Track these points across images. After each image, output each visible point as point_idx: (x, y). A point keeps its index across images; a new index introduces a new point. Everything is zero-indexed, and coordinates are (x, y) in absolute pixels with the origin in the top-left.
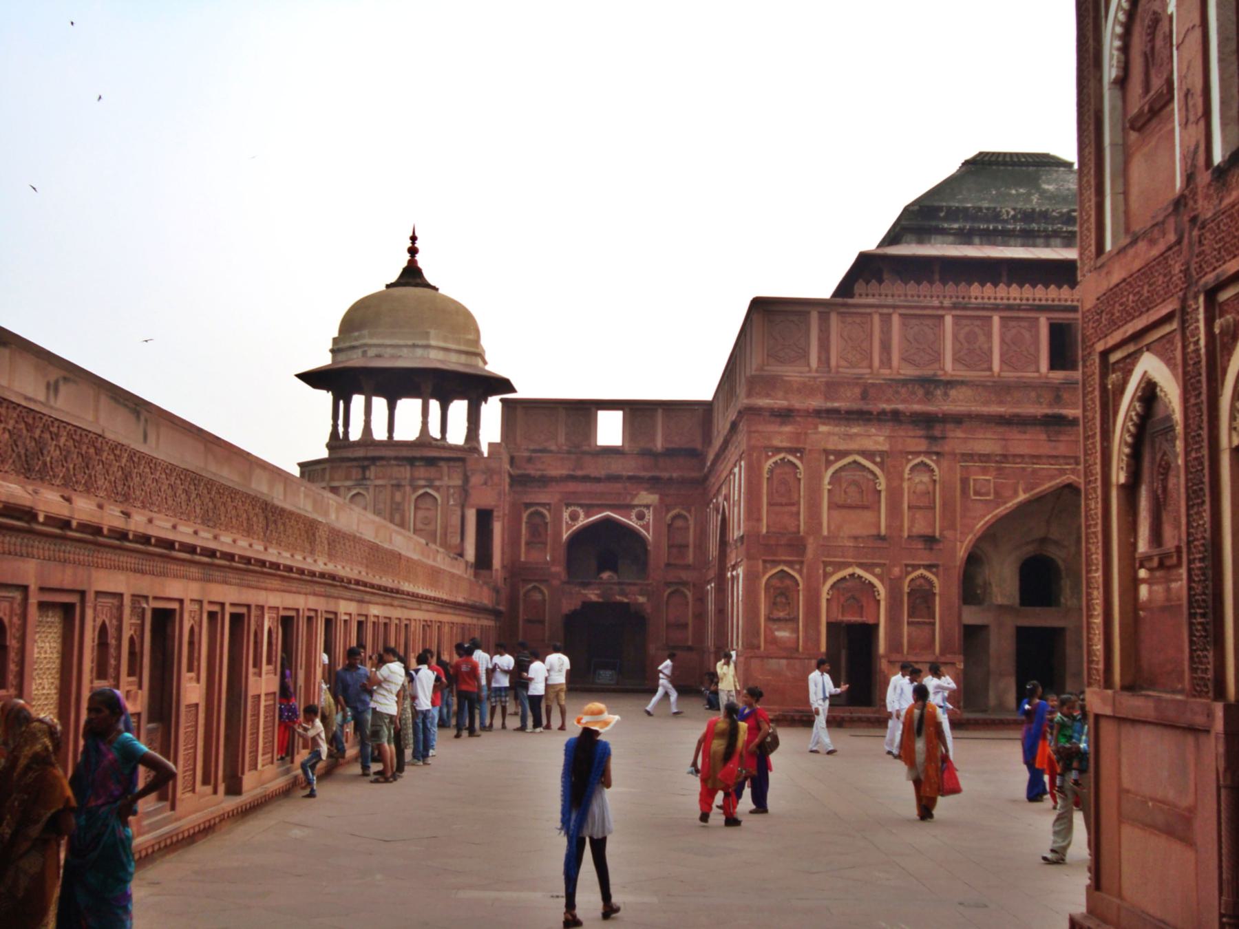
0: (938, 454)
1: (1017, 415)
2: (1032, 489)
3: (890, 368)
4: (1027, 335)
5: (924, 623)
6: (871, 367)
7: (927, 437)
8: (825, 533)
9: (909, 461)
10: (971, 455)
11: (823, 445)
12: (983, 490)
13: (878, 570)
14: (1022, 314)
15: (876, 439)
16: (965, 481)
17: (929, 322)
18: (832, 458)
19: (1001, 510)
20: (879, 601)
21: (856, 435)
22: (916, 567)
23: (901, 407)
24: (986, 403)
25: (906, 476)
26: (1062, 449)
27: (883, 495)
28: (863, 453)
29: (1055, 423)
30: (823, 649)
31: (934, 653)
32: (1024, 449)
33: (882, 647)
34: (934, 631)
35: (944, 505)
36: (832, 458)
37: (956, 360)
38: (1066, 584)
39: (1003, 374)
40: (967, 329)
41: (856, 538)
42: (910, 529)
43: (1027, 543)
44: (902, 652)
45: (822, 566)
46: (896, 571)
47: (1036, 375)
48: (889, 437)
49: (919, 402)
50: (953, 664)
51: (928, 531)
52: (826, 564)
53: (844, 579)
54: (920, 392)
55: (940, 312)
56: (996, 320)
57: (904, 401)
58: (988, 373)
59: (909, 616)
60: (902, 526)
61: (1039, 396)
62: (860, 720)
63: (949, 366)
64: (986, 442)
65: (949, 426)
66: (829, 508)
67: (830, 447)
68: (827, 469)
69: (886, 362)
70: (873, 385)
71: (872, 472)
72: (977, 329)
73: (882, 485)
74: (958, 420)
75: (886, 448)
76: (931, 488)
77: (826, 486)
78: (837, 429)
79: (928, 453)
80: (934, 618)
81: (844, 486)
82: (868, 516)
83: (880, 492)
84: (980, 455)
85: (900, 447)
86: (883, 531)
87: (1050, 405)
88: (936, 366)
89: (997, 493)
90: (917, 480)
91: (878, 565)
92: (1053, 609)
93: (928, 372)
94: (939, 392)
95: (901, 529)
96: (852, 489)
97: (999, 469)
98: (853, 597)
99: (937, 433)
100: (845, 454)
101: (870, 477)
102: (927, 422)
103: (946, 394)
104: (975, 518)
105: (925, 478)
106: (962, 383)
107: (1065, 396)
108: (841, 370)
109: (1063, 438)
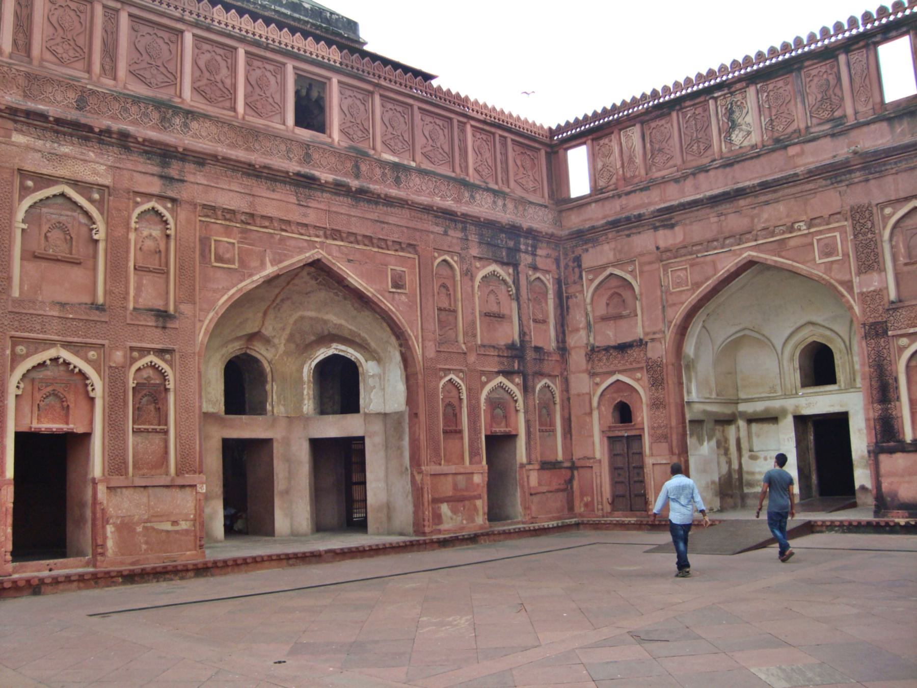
0: (173, 200)
1: (265, 167)
2: (281, 262)
3: (115, 79)
4: (272, 80)
5: (155, 431)
6: (89, 71)
7: (161, 177)
8: (16, 293)
9: (137, 204)
10: (213, 208)
11: (17, 163)
12: (228, 256)
13: (92, 354)
14: (268, 54)
15: (96, 166)
16: (204, 242)
17: (166, 35)
18: (30, 183)
19: (248, 284)
20: (92, 400)
21: (66, 156)
22: (144, 351)
23: (131, 129)
24: (233, 146)
25: (133, 225)
26: (311, 218)
27: (101, 246)
28: (75, 184)
29: (305, 183)
30: (10, 473)
31: (167, 473)
32: (271, 211)
33: (97, 466)
34: (166, 442)
35: (181, 269)
36: (30, 183)
37: (195, 89)
38: (273, 389)
39: (247, 118)
40: (208, 56)
41: (63, 305)
42: (136, 301)
43: (238, 338)
44: (127, 473)
45: (9, 343)
46: (118, 356)
47: (282, 127)
48: (111, 167)
49: (152, 128)
50: (193, 486)
51: (159, 304)
52: (15, 341)
53: (42, 365)
54: (155, 115)
55: (179, 26)
56: (241, 52)
57: (133, 123)
58: (233, 114)
59: (134, 423)
60: (127, 293)
61: (288, 151)
62: (68, 579)
63: (187, 93)
64: (230, 195)
65: (190, 167)
66: (22, 259)
67: (28, 167)
68: (22, 198)
69: (110, 69)
70: (93, 92)
71: (86, 213)
72: (219, 58)
73: (100, 235)
74: (201, 160)
75: (107, 181)
76: (162, 247)
77: (19, 224)
78: (39, 143)
79: (161, 198)
80: (166, 424)
81: (45, 228)
82: (77, 274)
83: (97, 241)
84: (224, 210)
85: (126, 184)
86: (100, 300)
87: (300, 163)
88: (171, 91)
89: (242, 262)
90: (145, 233)
91: (92, 346)
92: (260, 418)
93: (163, 94)
94: (177, 121)
95: (125, 298)
96: (56, 235)
97: (244, 231)
98: (55, 394)
99: (173, 172)
100: (50, 180)
101: (83, 220)
102: (164, 154)
103: (186, 125)
104: (214, 291)
105: (156, 232)
106: (206, 117)
107: (316, 156)
108: (46, 64)
109: (313, 204)
